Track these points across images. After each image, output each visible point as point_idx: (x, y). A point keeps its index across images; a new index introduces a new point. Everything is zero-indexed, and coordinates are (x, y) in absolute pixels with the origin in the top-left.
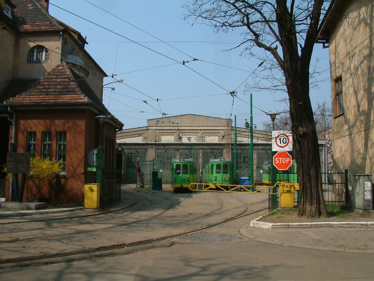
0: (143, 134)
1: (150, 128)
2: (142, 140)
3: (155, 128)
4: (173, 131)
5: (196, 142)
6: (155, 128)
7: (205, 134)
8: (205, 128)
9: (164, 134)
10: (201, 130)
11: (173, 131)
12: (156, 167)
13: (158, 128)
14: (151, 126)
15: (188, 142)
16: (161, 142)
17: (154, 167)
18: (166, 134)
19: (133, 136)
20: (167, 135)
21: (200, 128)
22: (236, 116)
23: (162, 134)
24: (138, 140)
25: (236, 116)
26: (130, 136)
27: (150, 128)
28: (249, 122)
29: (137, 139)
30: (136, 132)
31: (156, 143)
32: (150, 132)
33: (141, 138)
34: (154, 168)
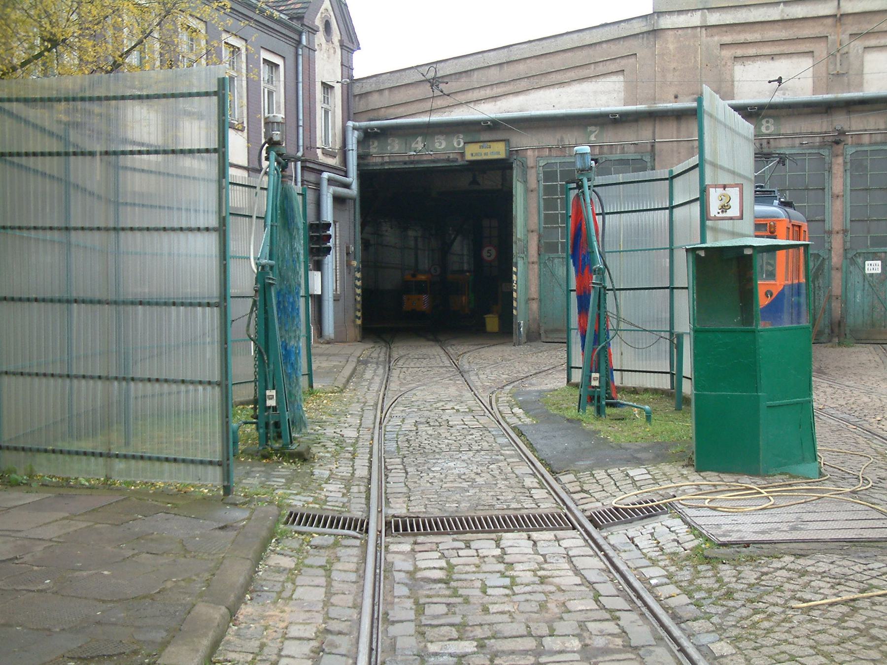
0: (632, 60)
1: (666, 22)
2: (622, 95)
3: (695, 19)
4: (807, 31)
6: (695, 19)
9: (752, 51)
11: (807, 31)
13: (714, 19)
14: (670, 13)
17: (714, 196)
18: (767, 50)
19: (572, 75)
20: (772, 57)
23: (739, 52)
24: (603, 99)
26: (554, 78)
27: (666, 22)
29: (595, 92)
30: (591, 51)
32: (670, 44)
34: (714, 210)
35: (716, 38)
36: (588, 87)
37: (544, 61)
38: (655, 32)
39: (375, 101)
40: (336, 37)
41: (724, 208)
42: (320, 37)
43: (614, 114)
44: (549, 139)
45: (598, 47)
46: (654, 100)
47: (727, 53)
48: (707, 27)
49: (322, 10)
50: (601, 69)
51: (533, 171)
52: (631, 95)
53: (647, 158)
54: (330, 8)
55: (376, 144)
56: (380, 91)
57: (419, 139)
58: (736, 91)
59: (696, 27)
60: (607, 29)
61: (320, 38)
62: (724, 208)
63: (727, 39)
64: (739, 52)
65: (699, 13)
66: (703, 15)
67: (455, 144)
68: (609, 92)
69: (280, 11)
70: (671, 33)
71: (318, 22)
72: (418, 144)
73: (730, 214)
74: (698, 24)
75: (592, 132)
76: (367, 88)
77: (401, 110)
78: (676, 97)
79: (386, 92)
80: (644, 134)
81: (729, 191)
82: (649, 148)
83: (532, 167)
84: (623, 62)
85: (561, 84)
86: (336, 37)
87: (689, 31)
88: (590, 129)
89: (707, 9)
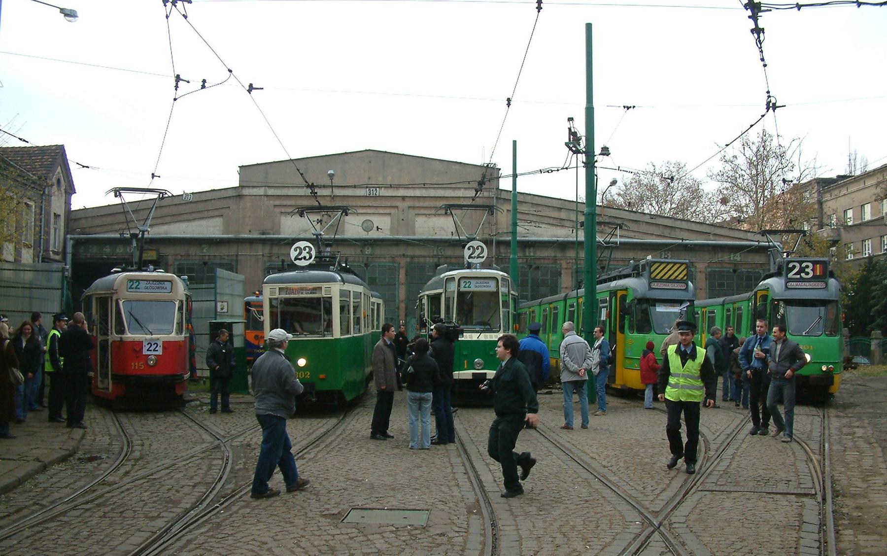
0: (227, 210)
1: (246, 192)
2: (222, 228)
3: (261, 191)
5: (385, 234)
6: (261, 191)
7: (417, 211)
8: (418, 193)
10: (404, 198)
12: (225, 304)
13: (271, 192)
15: (363, 235)
16: (280, 234)
17: (219, 304)
19: (193, 216)
21: (402, 192)
22: (515, 142)
23: (283, 210)
25: (515, 142)
26: (185, 217)
27: (246, 192)
28: (582, 132)
31: (264, 236)
32: (248, 203)
33: (218, 222)
34: (219, 309)
35: (271, 202)
36: (204, 223)
37: (180, 207)
38: (240, 197)
39: (84, 223)
40: (63, 188)
41: (222, 309)
42: (55, 188)
43: (216, 239)
44: (181, 250)
45: (209, 202)
46: (239, 232)
47: (277, 210)
48: (268, 196)
49: (56, 173)
50: (211, 213)
51: (172, 267)
52: (226, 228)
53: (234, 263)
54: (61, 172)
55: (83, 248)
56: (86, 218)
57: (108, 246)
58: (281, 230)
59: (261, 195)
60: (214, 193)
61: (55, 188)
62: (222, 309)
63: (277, 203)
64: (283, 210)
65: (263, 188)
66: (265, 191)
67: (128, 250)
68: (215, 226)
69: (34, 174)
70: (249, 197)
71: (54, 180)
72: (108, 250)
73: (223, 311)
74: (262, 194)
75: (204, 248)
76: (79, 215)
77: (98, 229)
78: (250, 231)
79: (90, 219)
80: (233, 250)
81: (223, 303)
82: (235, 258)
83: (171, 265)
84: (224, 210)
85: (188, 220)
86: (63, 188)
87: (258, 197)
88: (204, 246)
89: (268, 187)
